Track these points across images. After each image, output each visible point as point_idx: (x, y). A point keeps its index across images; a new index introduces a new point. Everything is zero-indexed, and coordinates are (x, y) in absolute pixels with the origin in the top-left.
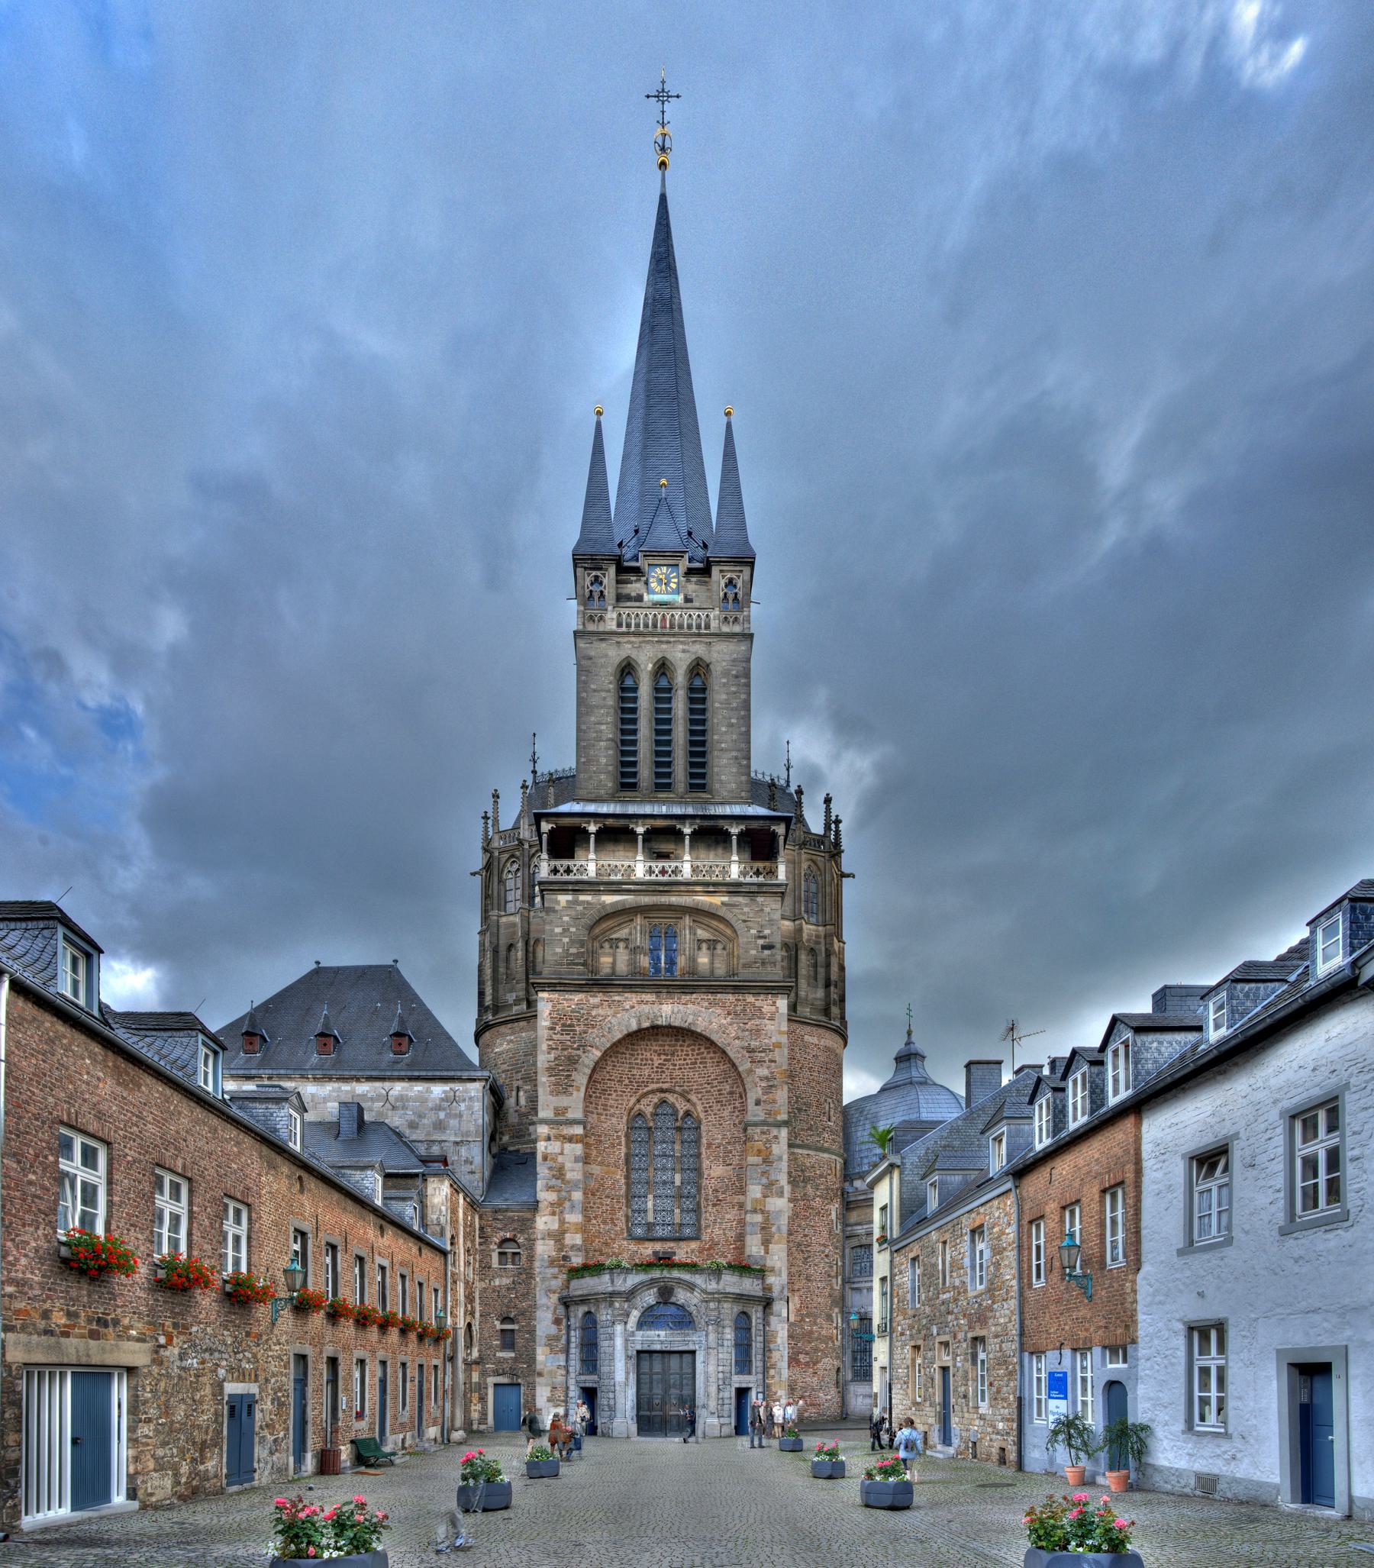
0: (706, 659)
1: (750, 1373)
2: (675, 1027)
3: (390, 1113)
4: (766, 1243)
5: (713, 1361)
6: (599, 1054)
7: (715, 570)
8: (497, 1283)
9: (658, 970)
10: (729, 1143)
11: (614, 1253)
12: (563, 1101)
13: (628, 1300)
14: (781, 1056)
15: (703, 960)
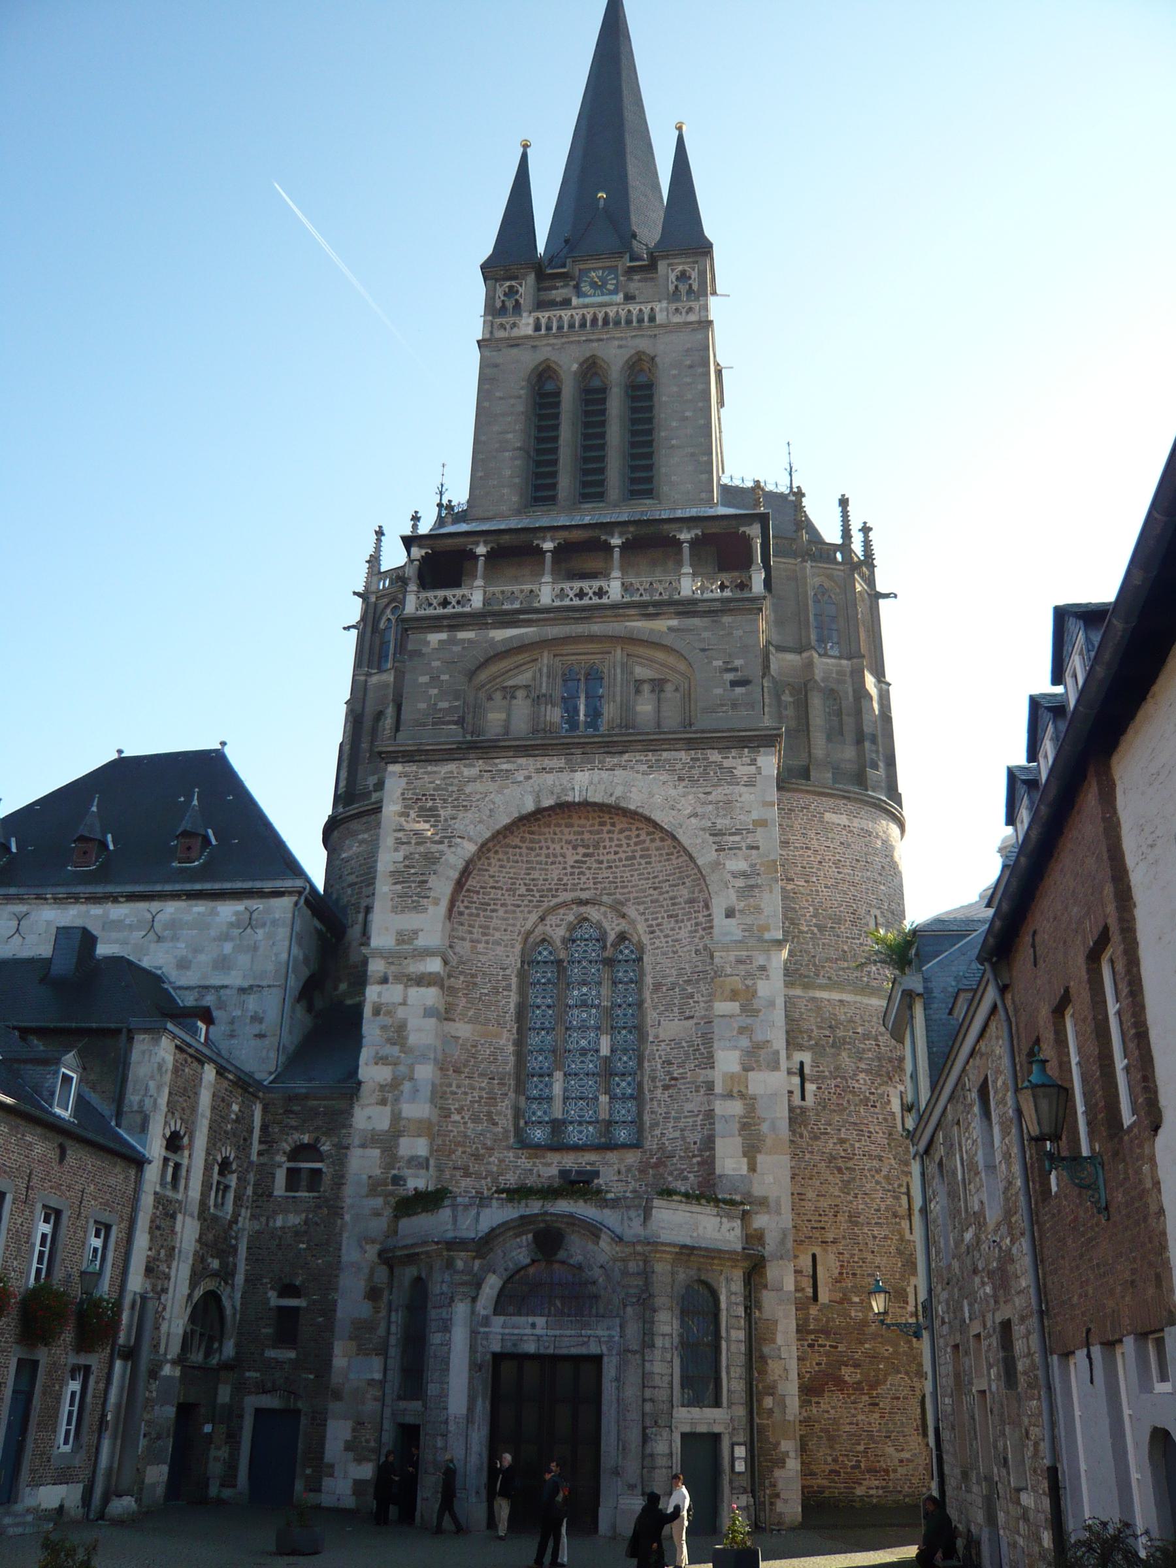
0: (650, 351)
1: (717, 1404)
2: (595, 804)
3: (153, 946)
4: (751, 1151)
5: (632, 1378)
6: (470, 848)
7: (662, 266)
8: (279, 1223)
9: (573, 724)
10: (688, 982)
11: (489, 1173)
12: (409, 921)
13: (480, 1255)
14: (768, 839)
15: (645, 707)
